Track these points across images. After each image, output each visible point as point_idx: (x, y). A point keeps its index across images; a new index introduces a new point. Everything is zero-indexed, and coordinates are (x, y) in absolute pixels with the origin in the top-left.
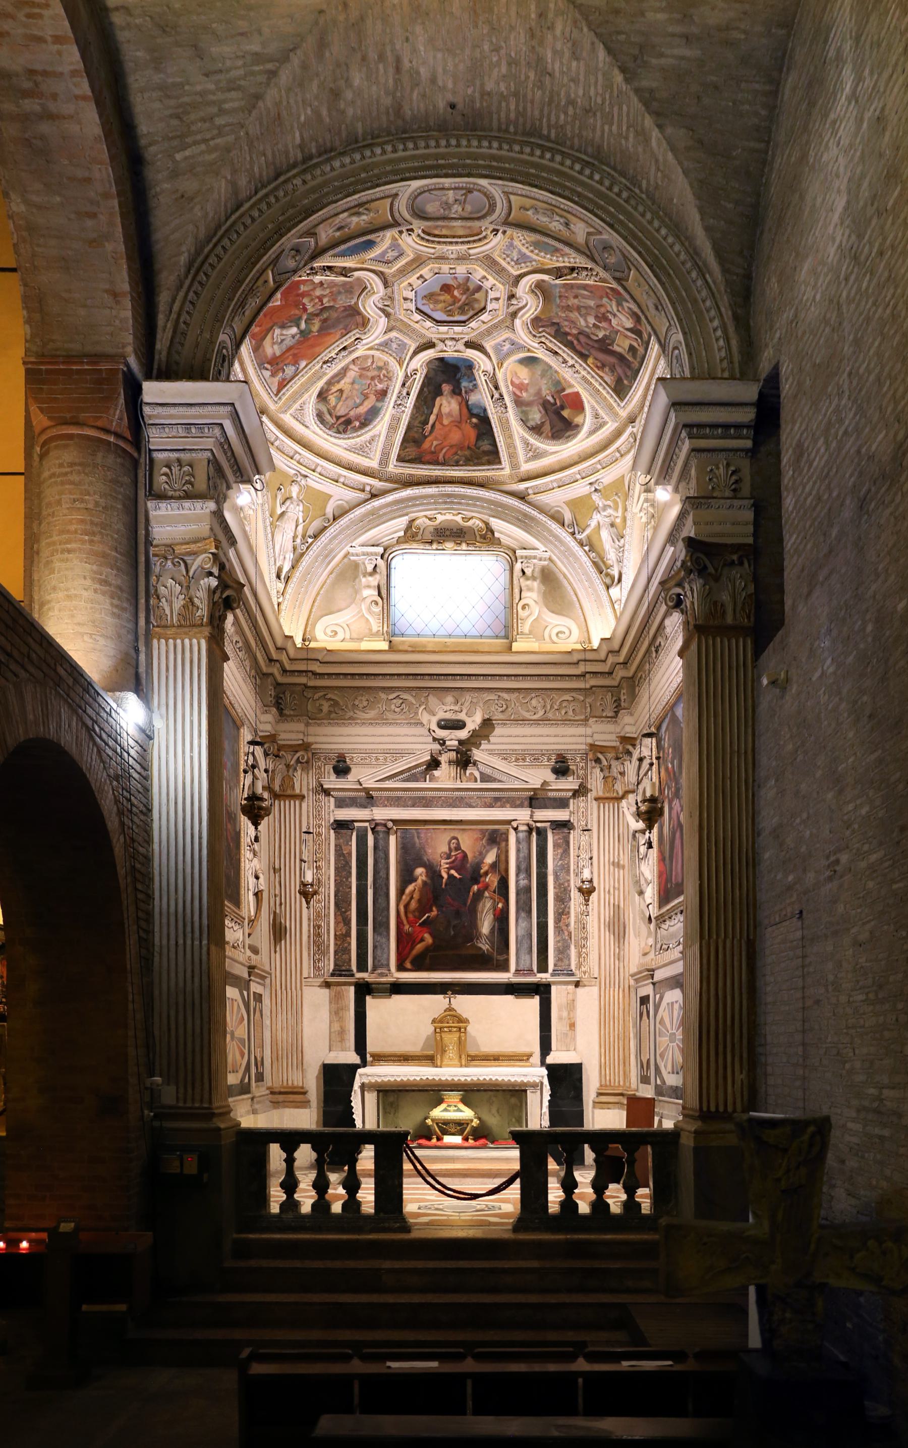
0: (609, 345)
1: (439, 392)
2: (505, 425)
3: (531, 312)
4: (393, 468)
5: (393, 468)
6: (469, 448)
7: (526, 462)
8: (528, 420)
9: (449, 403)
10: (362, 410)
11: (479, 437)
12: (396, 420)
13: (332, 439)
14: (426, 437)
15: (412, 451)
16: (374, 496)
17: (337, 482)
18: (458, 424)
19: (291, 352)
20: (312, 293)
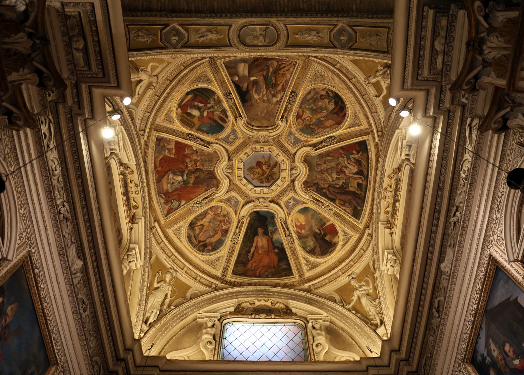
0: (346, 188)
1: (256, 234)
2: (294, 251)
3: (303, 177)
4: (230, 277)
5: (230, 277)
6: (274, 267)
7: (308, 271)
8: (306, 247)
9: (262, 240)
10: (214, 240)
11: (279, 261)
12: (232, 249)
13: (195, 253)
14: (249, 261)
15: (241, 269)
16: (216, 290)
17: (196, 279)
18: (267, 253)
19: (177, 192)
20: (191, 156)
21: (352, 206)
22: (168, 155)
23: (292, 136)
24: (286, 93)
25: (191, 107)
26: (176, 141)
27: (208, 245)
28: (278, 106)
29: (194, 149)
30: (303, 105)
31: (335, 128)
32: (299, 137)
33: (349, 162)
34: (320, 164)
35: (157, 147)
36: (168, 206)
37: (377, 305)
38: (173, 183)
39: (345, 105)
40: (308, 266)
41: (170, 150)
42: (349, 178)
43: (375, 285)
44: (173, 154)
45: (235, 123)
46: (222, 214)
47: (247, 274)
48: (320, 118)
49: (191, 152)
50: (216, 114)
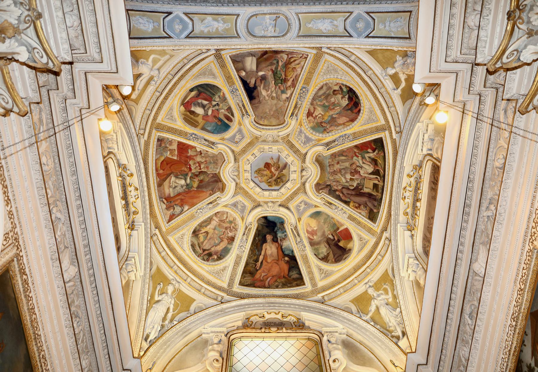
0: (361, 189)
1: (264, 241)
2: (305, 259)
4: (237, 288)
6: (284, 277)
7: (321, 280)
8: (319, 254)
9: (271, 247)
10: (220, 248)
11: (289, 270)
12: (239, 258)
14: (257, 270)
15: (249, 279)
17: (200, 291)
18: (277, 261)
19: (179, 197)
20: (195, 158)
21: (368, 208)
22: (171, 157)
23: (303, 135)
24: (296, 88)
25: (195, 105)
26: (178, 142)
27: (213, 253)
28: (288, 103)
29: (198, 150)
30: (315, 102)
31: (349, 125)
32: (310, 136)
33: (364, 161)
34: (333, 165)
35: (159, 148)
36: (170, 212)
37: (397, 316)
38: (176, 187)
39: (359, 100)
40: (321, 274)
41: (172, 151)
42: (364, 179)
43: (395, 293)
44: (175, 156)
45: (241, 122)
46: (227, 220)
47: (255, 285)
48: (332, 115)
49: (195, 154)
50: (222, 112)
